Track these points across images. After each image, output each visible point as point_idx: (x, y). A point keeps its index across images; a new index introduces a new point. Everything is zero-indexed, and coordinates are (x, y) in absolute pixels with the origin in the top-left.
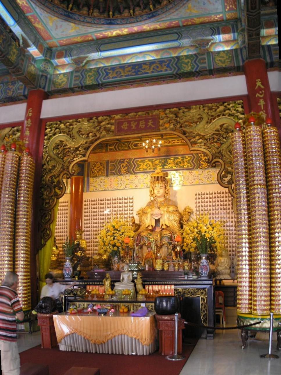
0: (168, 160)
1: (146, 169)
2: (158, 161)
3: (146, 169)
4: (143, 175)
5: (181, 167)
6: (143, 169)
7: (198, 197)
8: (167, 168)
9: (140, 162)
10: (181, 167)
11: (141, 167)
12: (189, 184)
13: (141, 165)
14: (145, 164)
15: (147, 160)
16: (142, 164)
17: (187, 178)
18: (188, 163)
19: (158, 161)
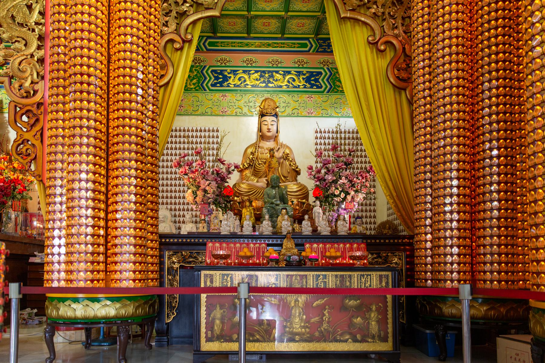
0: (274, 74)
1: (238, 86)
2: (259, 74)
3: (238, 86)
4: (234, 94)
5: (295, 87)
6: (234, 85)
7: (319, 135)
8: (272, 87)
9: (229, 73)
10: (295, 87)
11: (231, 81)
12: (307, 115)
13: (230, 77)
14: (238, 76)
15: (241, 71)
16: (232, 76)
17: (304, 105)
18: (306, 82)
19: (259, 74)
